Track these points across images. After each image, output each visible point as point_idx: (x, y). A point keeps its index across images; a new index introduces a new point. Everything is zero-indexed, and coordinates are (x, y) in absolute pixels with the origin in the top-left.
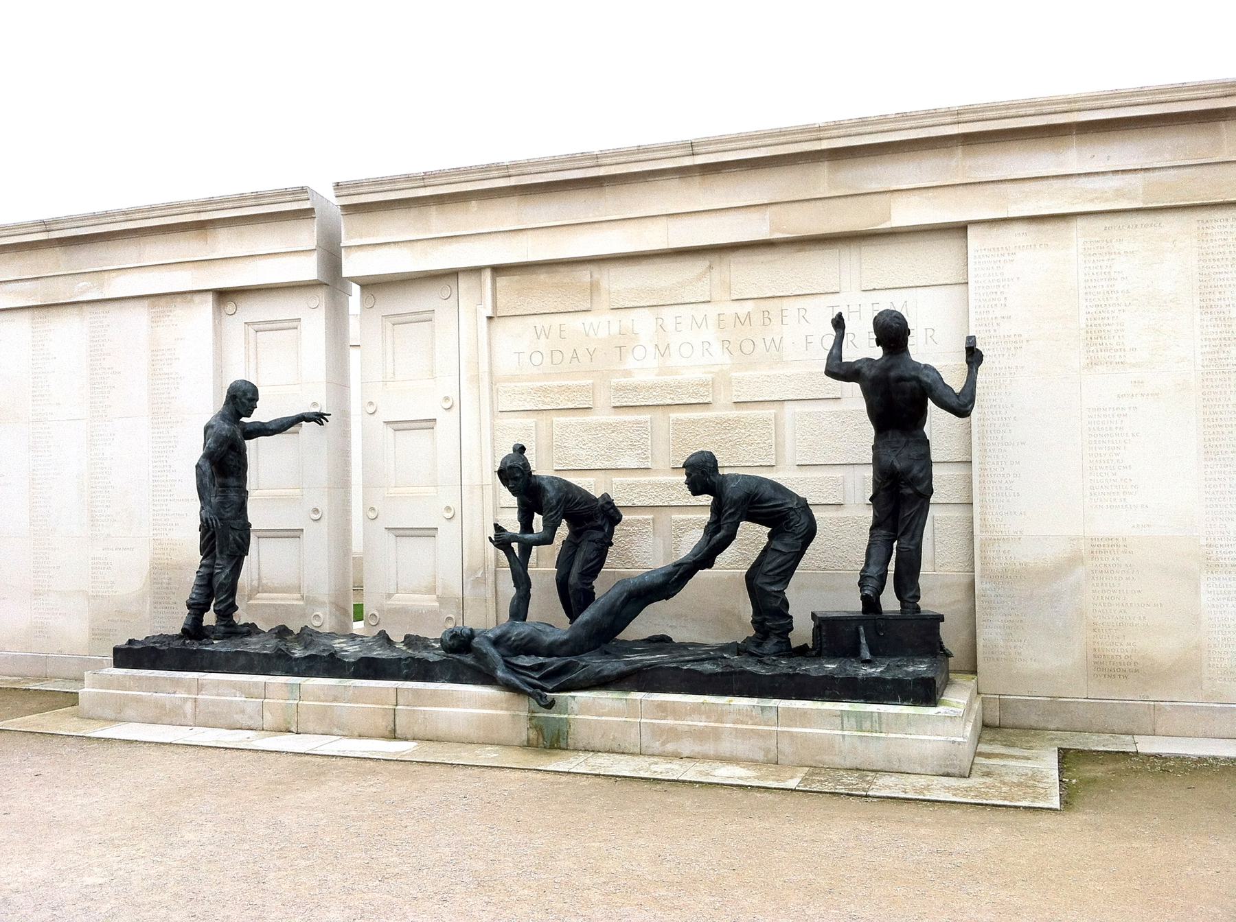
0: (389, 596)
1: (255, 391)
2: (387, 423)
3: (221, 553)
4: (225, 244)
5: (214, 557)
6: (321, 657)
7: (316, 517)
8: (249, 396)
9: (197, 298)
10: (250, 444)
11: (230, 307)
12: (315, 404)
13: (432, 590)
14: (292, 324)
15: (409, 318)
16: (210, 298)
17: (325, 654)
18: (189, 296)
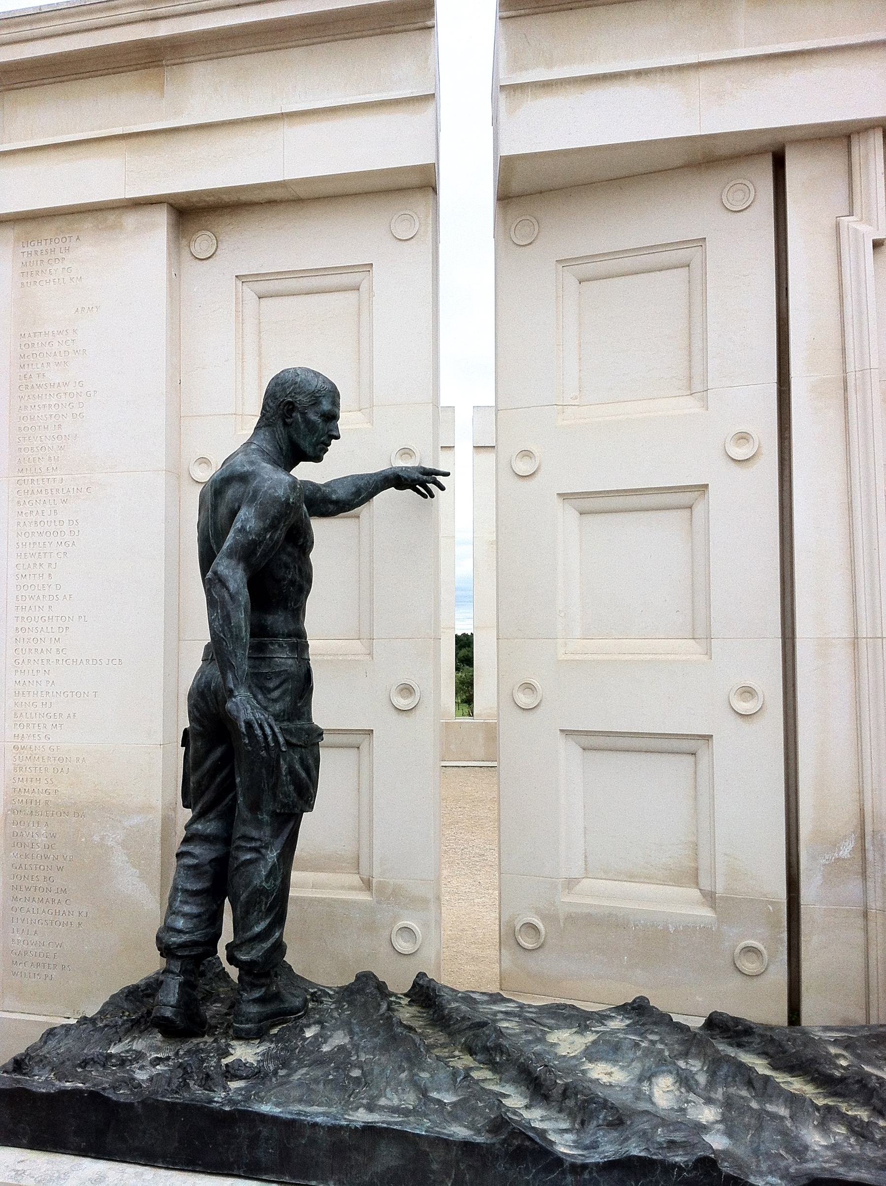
0: (571, 883)
1: (334, 395)
2: (564, 496)
3: (255, 807)
4: (204, 94)
5: (228, 817)
6: (668, 1168)
7: (403, 703)
8: (326, 406)
9: (131, 220)
10: (319, 527)
11: (202, 243)
12: (406, 452)
13: (693, 877)
14: (351, 279)
15: (627, 263)
16: (161, 218)
17: (679, 1158)
18: (112, 217)
